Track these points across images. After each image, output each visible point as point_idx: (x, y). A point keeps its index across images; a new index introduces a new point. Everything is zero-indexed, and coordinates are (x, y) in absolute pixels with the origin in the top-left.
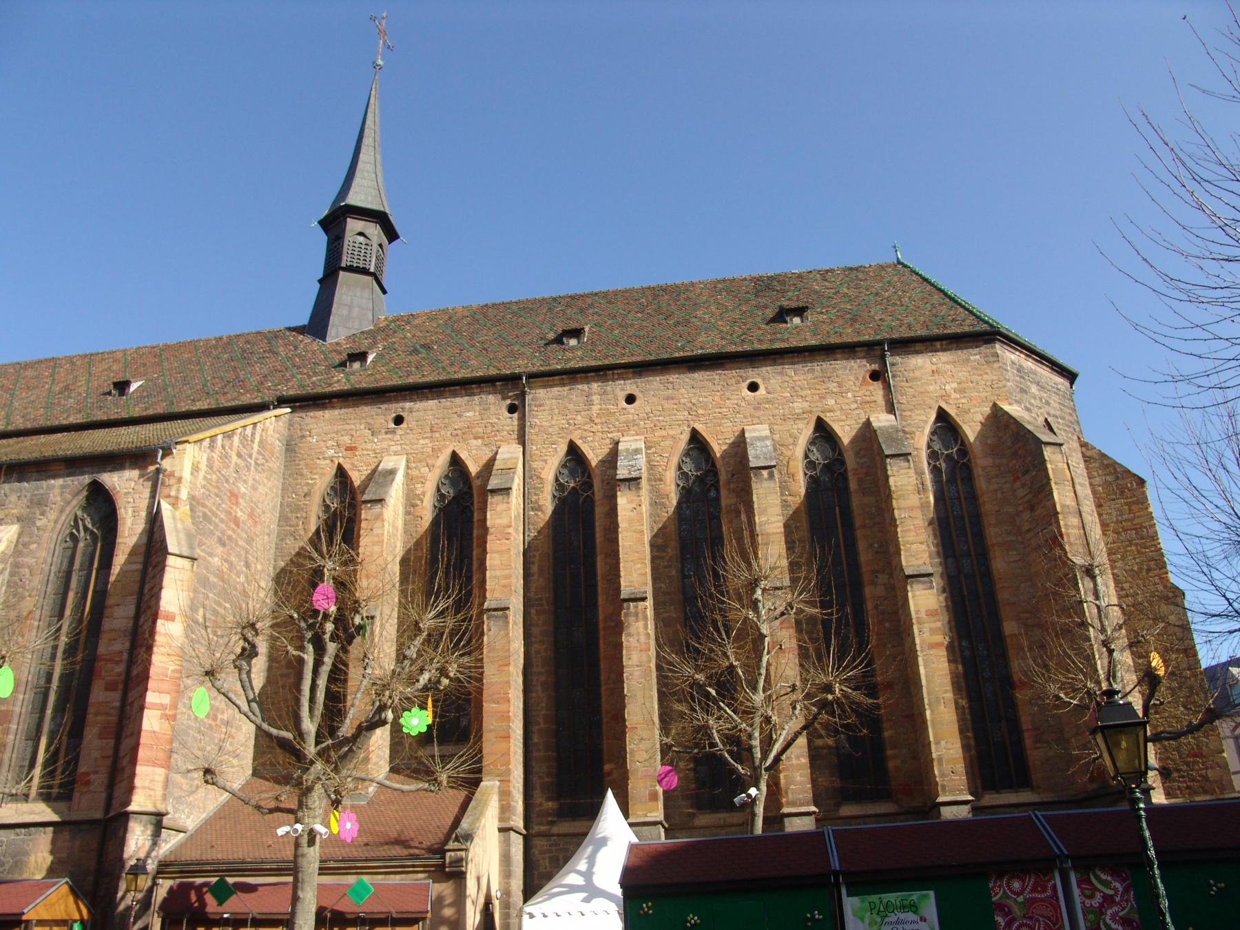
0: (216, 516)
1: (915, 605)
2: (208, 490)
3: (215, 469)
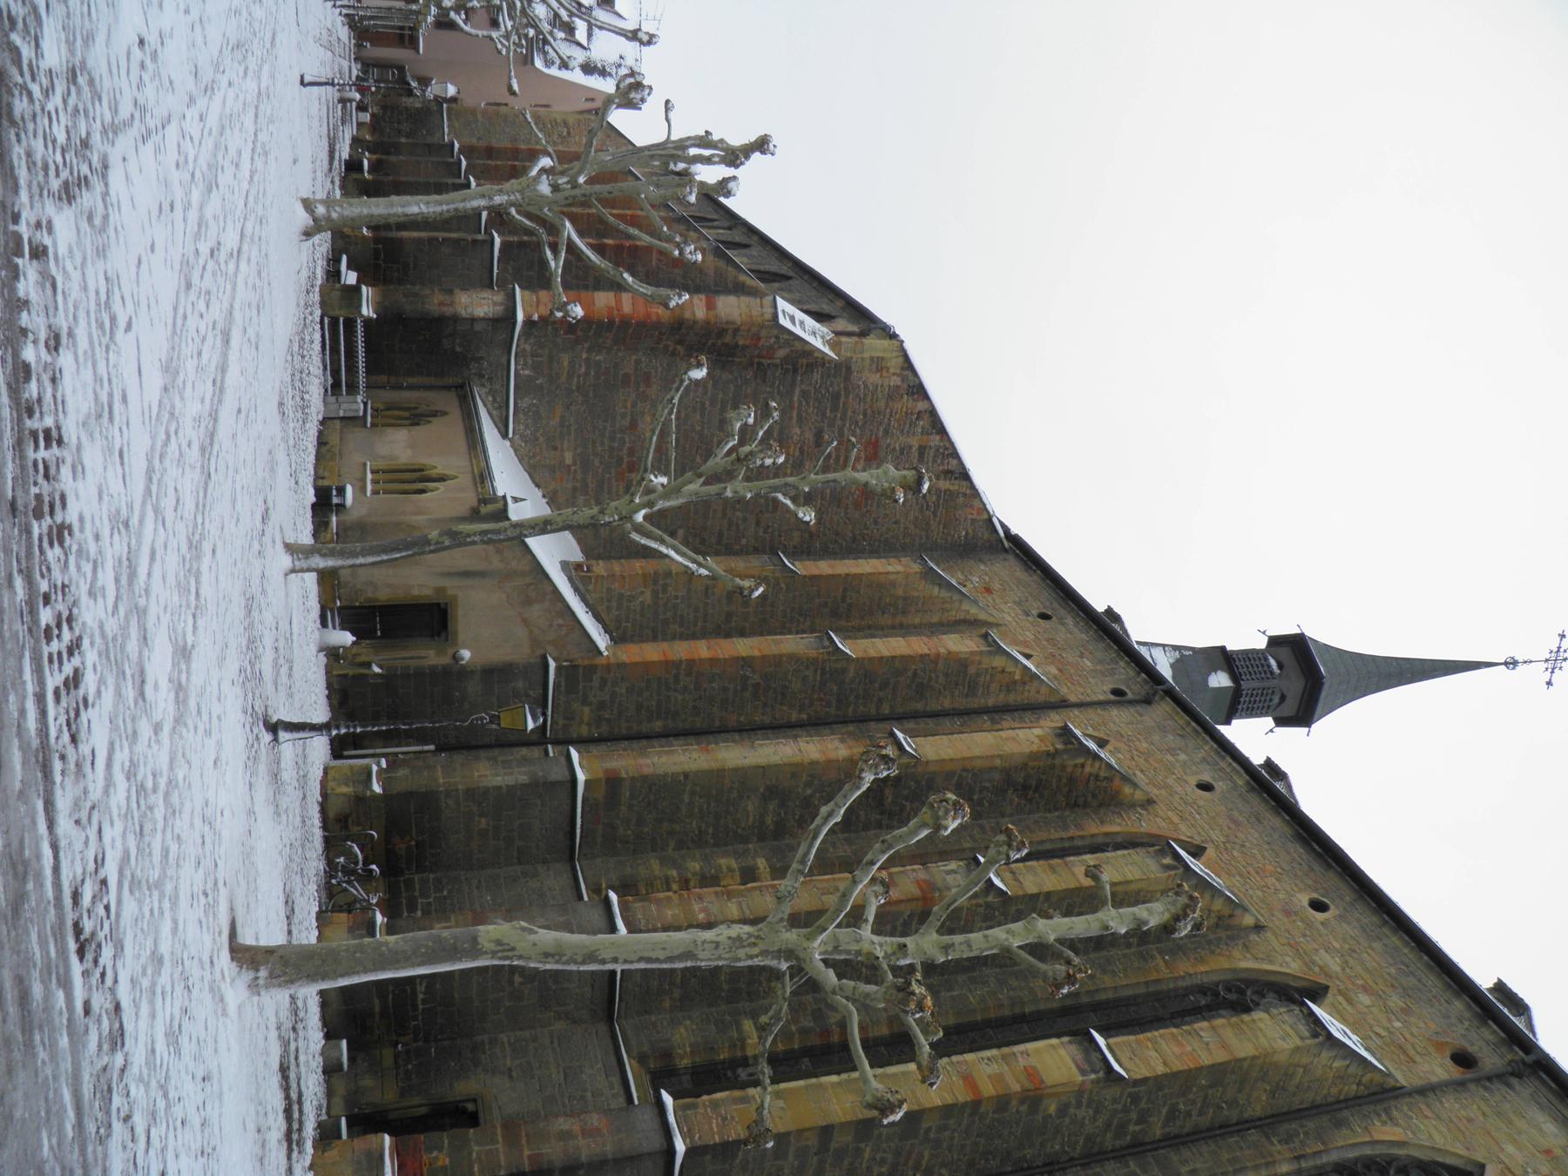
0: (843, 419)
1: (1037, 1051)
2: (865, 395)
3: (891, 404)
